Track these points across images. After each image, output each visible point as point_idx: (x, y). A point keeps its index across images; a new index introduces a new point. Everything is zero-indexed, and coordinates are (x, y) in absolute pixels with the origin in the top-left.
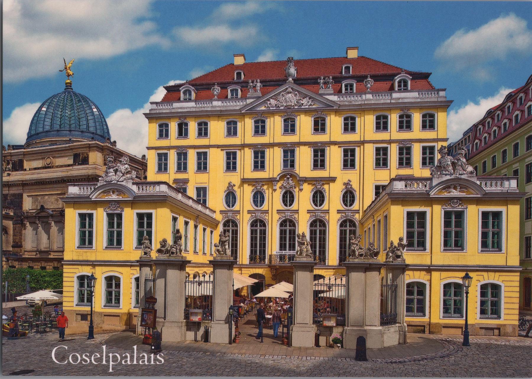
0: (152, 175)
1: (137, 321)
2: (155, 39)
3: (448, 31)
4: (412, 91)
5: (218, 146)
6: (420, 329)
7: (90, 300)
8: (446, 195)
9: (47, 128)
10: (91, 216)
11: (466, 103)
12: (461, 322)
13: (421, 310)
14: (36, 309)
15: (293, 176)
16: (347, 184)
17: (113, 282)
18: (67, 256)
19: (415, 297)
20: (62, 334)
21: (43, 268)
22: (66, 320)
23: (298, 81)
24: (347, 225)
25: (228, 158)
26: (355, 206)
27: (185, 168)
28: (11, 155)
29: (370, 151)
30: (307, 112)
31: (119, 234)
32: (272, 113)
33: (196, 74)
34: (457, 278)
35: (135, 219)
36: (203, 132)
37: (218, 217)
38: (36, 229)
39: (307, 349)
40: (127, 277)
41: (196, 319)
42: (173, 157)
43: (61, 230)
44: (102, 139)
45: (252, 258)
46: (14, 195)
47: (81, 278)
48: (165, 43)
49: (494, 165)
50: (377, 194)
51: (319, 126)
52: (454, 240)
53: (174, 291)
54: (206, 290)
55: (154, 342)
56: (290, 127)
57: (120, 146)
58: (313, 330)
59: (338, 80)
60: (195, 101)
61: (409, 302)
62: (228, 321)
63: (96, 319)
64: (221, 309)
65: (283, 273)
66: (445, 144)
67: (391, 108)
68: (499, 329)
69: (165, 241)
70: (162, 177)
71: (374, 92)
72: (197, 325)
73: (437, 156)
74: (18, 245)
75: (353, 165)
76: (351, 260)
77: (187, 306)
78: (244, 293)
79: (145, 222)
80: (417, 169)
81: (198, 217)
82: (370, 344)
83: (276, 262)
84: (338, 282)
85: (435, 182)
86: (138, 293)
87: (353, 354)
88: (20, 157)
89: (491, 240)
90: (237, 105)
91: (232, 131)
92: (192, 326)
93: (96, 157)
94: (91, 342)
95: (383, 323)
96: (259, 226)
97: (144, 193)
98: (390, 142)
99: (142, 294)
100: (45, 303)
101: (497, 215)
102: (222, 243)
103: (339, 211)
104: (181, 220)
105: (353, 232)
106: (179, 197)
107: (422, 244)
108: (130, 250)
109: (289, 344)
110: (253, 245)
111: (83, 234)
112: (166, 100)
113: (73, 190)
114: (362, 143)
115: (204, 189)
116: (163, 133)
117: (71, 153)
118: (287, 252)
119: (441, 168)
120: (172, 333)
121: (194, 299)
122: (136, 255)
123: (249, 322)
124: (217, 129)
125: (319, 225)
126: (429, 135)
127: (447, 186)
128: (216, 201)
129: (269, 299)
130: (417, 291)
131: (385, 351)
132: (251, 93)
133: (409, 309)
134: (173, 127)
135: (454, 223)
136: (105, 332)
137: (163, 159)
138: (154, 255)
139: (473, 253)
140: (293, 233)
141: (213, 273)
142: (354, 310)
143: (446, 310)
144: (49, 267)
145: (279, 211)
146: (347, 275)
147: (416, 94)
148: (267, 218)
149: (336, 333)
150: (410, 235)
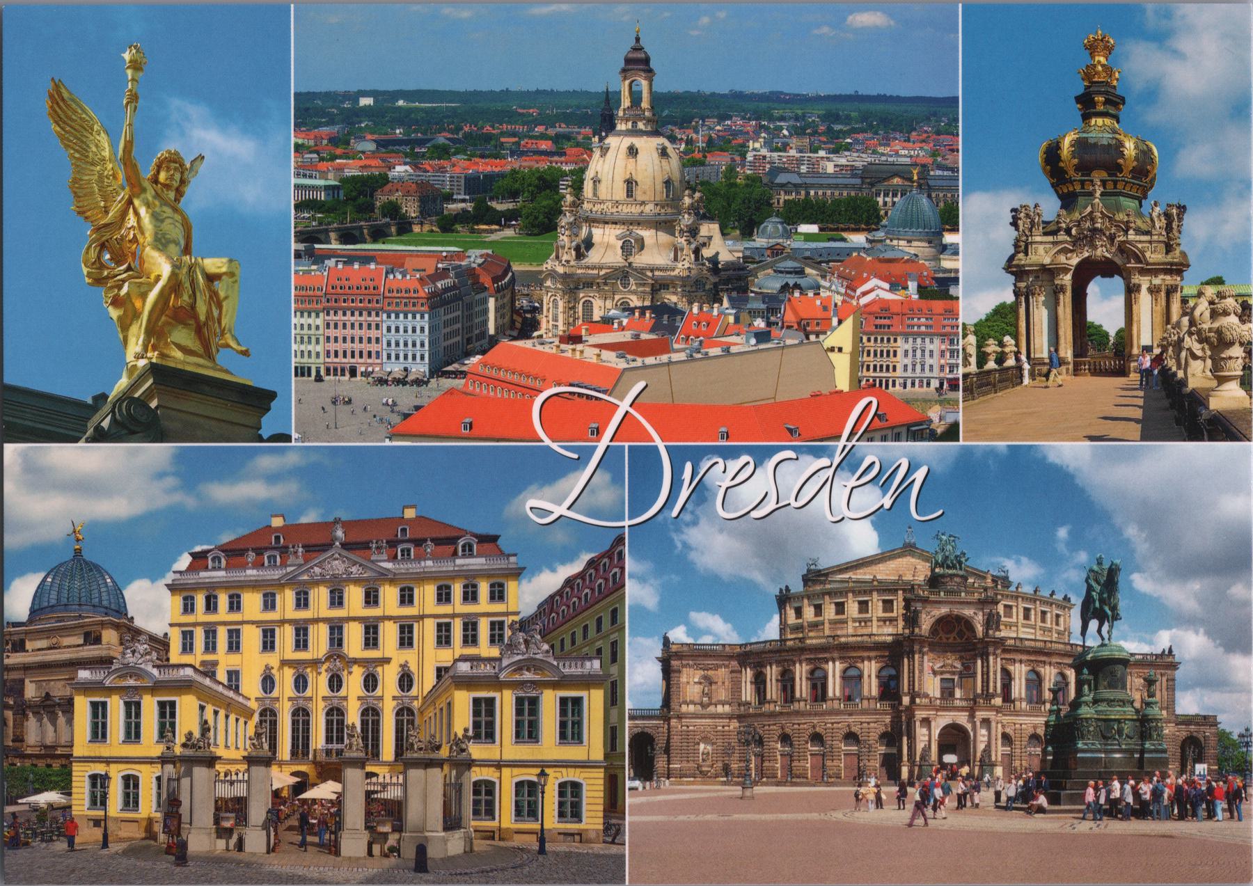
0: (175, 656)
1: (158, 828)
2: (177, 498)
3: (518, 487)
4: (479, 556)
5: (253, 623)
6: (489, 835)
7: (104, 803)
8: (517, 677)
9: (53, 602)
10: (104, 704)
11: (541, 571)
12: (536, 826)
13: (490, 813)
14: (41, 814)
15: (341, 657)
16: (404, 666)
17: (131, 783)
18: (77, 751)
19: (483, 797)
20: (71, 843)
21: (49, 766)
22: (76, 826)
23: (344, 546)
24: (405, 714)
25: (265, 636)
26: (414, 692)
27: (214, 648)
28: (10, 634)
29: (430, 627)
30: (357, 581)
31: (138, 726)
32: (317, 583)
33: (226, 538)
34: (531, 775)
35: (156, 709)
36: (235, 605)
37: (253, 705)
38: (40, 720)
39: (358, 859)
40: (147, 777)
41: (227, 824)
42: (199, 635)
43: (70, 721)
44: (118, 615)
45: (294, 753)
46: (14, 680)
47: (94, 778)
48: (190, 502)
49: (573, 643)
50: (439, 677)
51: (371, 598)
52: (528, 730)
53: (201, 791)
54: (240, 790)
55: (179, 852)
56: (337, 600)
57: (139, 623)
58: (365, 837)
59: (393, 544)
60: (226, 569)
61: (476, 803)
62: (265, 827)
63: (110, 825)
64: (258, 812)
65: (330, 771)
66: (517, 618)
67: (455, 576)
68: (580, 835)
69: (190, 734)
70: (187, 659)
71: (435, 557)
72: (229, 832)
73: (508, 633)
74: (19, 739)
75: (410, 644)
76: (409, 755)
77: (217, 809)
78: (285, 794)
79: (167, 711)
80: (485, 648)
81: (229, 705)
82: (433, 852)
83: (322, 757)
84: (394, 780)
85: (505, 663)
86: (159, 795)
87: (412, 864)
88: (22, 636)
89: (571, 730)
90: (276, 574)
91: (269, 604)
92: (223, 833)
93: (110, 636)
94: (105, 852)
95: (446, 829)
96: (301, 716)
97: (162, 678)
98: (454, 616)
99: (164, 796)
100: (51, 806)
101: (577, 702)
102: (258, 735)
103: (394, 698)
104: (210, 709)
105: (411, 722)
106: (207, 682)
107: (490, 736)
108: (150, 745)
109: (337, 853)
110: (294, 739)
111: (95, 726)
112: (191, 568)
113: (84, 674)
114: (422, 617)
115: (237, 673)
116: (189, 607)
117: (82, 631)
118: (335, 746)
119: (511, 647)
120: (200, 841)
121: (226, 801)
122: (158, 750)
123: (290, 828)
124: (252, 602)
125: (371, 714)
126: (498, 607)
127: (519, 667)
128: (251, 687)
129: (314, 801)
130: (486, 790)
131: (449, 860)
132: (292, 560)
133: (476, 813)
134: (200, 600)
135: (528, 711)
136: (121, 840)
137: (188, 637)
138: (178, 750)
139: (549, 746)
140: (341, 723)
141: (248, 770)
142: (413, 813)
143: (518, 812)
144: (56, 765)
145: (324, 698)
146: (404, 773)
147: (482, 560)
148: (311, 706)
149: (392, 840)
150: (476, 725)
